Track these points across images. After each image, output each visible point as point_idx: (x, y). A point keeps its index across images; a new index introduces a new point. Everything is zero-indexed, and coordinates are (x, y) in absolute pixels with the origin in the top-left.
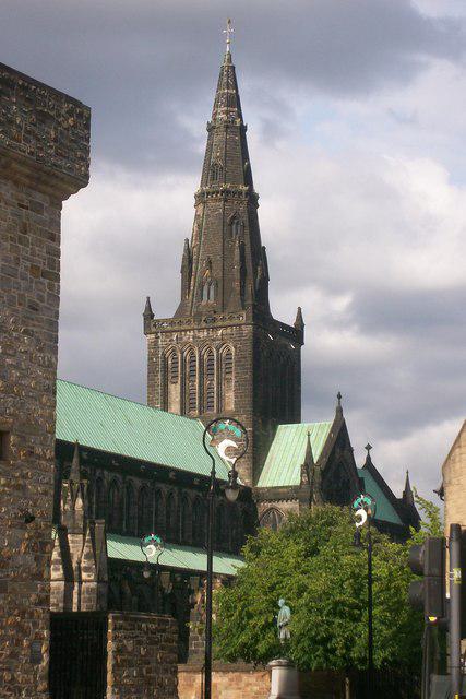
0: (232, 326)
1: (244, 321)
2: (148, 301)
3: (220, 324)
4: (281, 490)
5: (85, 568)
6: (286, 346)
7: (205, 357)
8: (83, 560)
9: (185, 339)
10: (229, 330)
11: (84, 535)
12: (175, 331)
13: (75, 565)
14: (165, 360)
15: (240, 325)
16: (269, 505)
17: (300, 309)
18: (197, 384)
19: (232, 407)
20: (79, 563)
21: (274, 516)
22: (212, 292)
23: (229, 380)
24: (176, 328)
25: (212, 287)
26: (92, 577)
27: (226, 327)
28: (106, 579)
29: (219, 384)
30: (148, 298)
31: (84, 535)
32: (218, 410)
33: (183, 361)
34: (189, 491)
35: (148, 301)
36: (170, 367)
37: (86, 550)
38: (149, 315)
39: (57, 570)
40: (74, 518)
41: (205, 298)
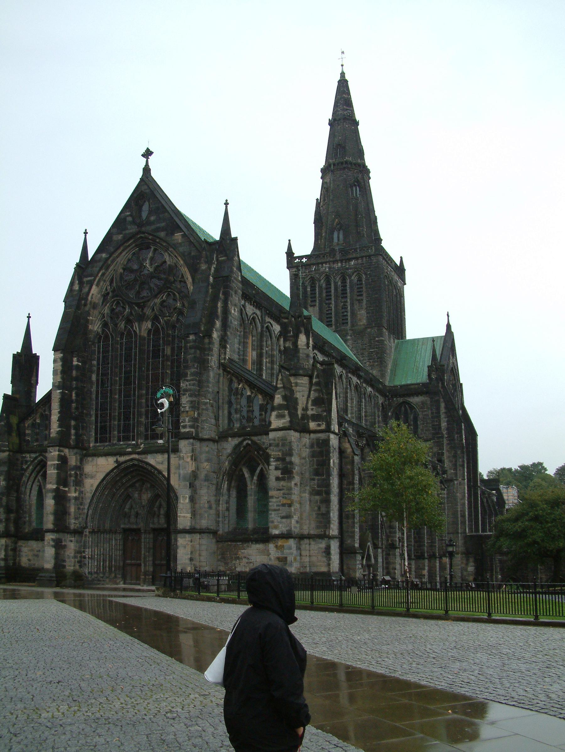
0: (362, 257)
1: (373, 253)
2: (290, 244)
3: (351, 256)
4: (412, 387)
5: (313, 415)
6: (396, 282)
7: (339, 283)
8: (310, 406)
9: (322, 270)
10: (360, 261)
11: (311, 377)
12: (314, 264)
13: (300, 412)
14: (305, 288)
15: (369, 256)
16: (401, 400)
17: (401, 258)
18: (333, 306)
19: (364, 322)
20: (305, 409)
21: (406, 409)
22: (341, 236)
23: (360, 301)
24: (314, 262)
25: (341, 232)
26: (323, 427)
27: (357, 259)
28: (337, 431)
29: (352, 305)
30: (289, 240)
31: (311, 377)
32: (353, 325)
33: (320, 287)
34: (352, 377)
35: (290, 244)
36: (309, 293)
37: (313, 395)
38: (290, 253)
39: (280, 416)
40: (298, 357)
41: (335, 240)
